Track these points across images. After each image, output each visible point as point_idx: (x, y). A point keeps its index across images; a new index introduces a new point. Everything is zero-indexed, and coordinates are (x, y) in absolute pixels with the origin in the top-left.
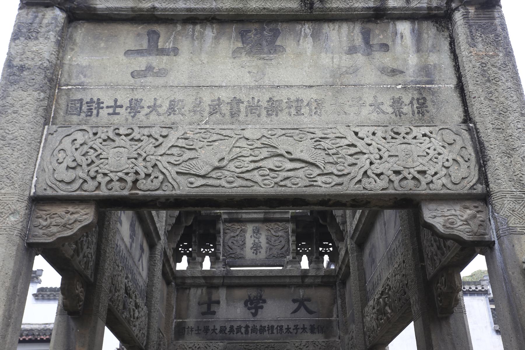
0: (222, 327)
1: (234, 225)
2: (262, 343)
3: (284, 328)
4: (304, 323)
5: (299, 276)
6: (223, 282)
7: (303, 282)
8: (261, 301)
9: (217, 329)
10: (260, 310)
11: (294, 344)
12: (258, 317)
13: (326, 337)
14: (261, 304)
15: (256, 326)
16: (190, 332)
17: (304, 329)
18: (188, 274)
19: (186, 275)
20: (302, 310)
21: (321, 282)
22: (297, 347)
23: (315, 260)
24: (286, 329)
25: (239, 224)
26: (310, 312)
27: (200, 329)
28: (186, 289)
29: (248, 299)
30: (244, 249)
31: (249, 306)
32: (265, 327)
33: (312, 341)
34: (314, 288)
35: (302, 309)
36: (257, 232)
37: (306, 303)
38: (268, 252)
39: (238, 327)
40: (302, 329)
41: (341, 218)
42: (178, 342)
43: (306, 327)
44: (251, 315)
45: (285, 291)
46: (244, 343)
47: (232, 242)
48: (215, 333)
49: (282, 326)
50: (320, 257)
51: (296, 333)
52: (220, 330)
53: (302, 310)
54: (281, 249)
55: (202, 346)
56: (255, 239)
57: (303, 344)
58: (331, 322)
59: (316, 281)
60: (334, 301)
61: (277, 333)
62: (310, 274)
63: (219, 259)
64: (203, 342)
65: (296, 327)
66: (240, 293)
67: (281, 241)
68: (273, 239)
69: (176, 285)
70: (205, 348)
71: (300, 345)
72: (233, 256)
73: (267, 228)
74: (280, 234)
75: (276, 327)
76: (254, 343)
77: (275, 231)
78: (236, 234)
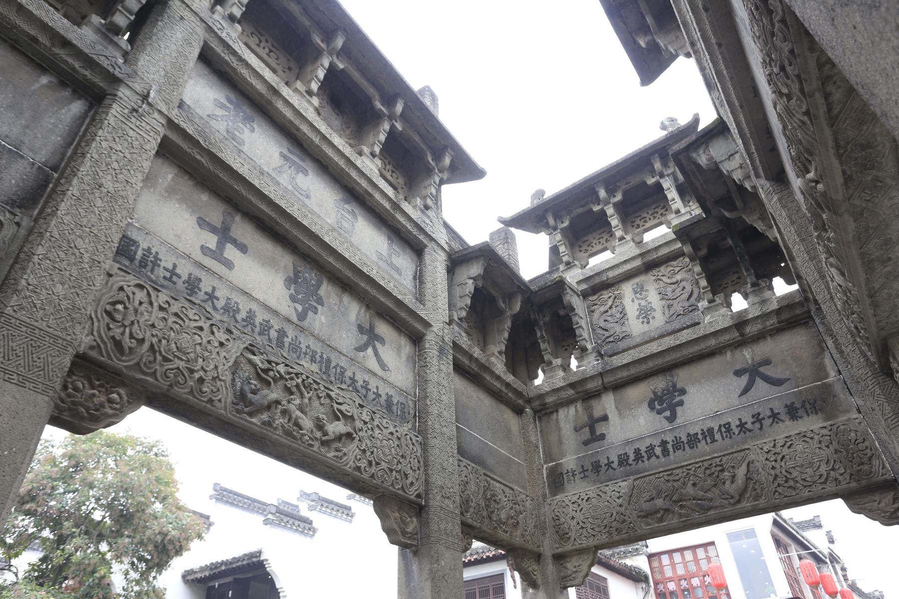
0: (621, 455)
1: (602, 295)
2: (696, 463)
3: (733, 426)
4: (770, 406)
5: (731, 327)
6: (603, 384)
7: (742, 335)
8: (676, 394)
9: (613, 462)
10: (679, 409)
11: (762, 449)
12: (679, 421)
13: (829, 416)
14: (678, 399)
15: (680, 438)
16: (572, 478)
17: (774, 416)
18: (546, 389)
19: (542, 392)
20: (759, 383)
21: (779, 323)
22: (767, 453)
23: (751, 290)
24: (737, 426)
25: (610, 290)
26: (776, 382)
27: (585, 469)
28: (552, 413)
29: (653, 396)
30: (626, 322)
31: (658, 407)
32: (697, 434)
33: (798, 432)
34: (769, 338)
35: (758, 380)
36: (640, 290)
37: (762, 369)
38: (666, 313)
39: (647, 448)
40: (769, 417)
41: (739, 171)
42: (555, 498)
43: (776, 411)
44: (667, 425)
45: (717, 361)
46: (663, 472)
47: (605, 321)
48: (612, 468)
49: (729, 423)
50: (760, 281)
51: (761, 429)
52: (619, 461)
53: (759, 383)
54: (689, 299)
55: (591, 495)
56: (640, 301)
57: (781, 443)
58: (827, 388)
59: (768, 323)
60: (821, 347)
61: (723, 439)
62: (750, 316)
63: (587, 350)
64: (593, 488)
65: (758, 418)
66: (640, 392)
67: (684, 288)
68: (669, 289)
69: (536, 412)
70: (598, 497)
71: (774, 446)
72: (611, 339)
73: (654, 278)
74: (678, 277)
75: (716, 429)
76: (682, 467)
77: (669, 278)
78: (608, 306)
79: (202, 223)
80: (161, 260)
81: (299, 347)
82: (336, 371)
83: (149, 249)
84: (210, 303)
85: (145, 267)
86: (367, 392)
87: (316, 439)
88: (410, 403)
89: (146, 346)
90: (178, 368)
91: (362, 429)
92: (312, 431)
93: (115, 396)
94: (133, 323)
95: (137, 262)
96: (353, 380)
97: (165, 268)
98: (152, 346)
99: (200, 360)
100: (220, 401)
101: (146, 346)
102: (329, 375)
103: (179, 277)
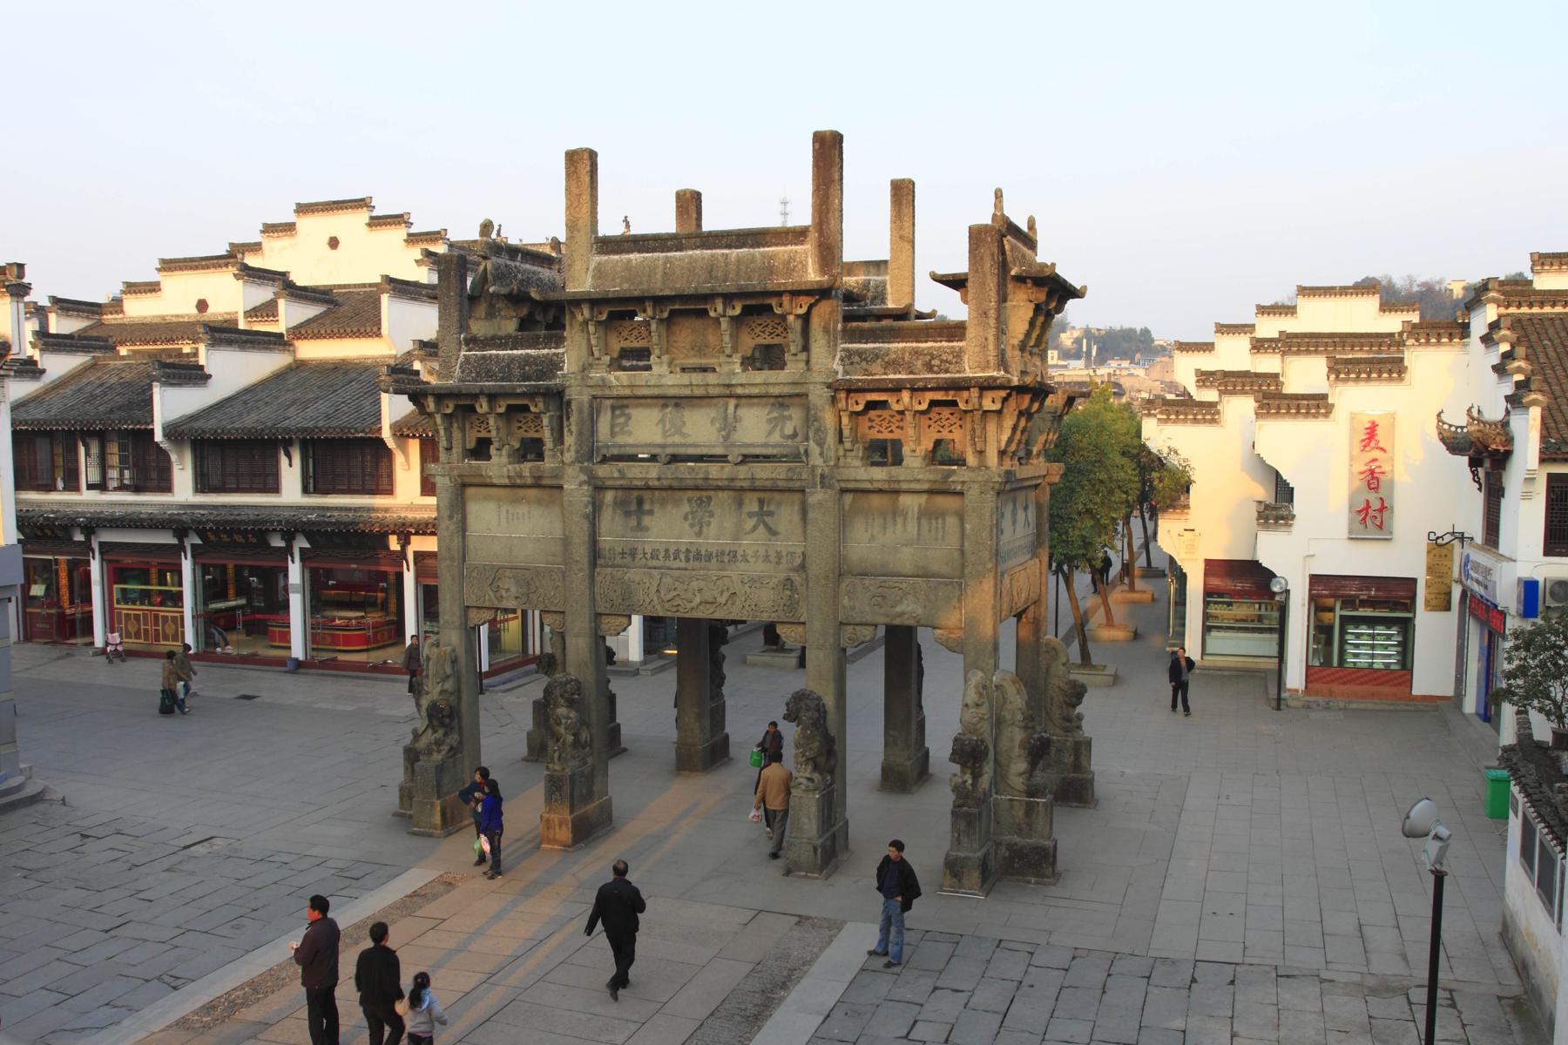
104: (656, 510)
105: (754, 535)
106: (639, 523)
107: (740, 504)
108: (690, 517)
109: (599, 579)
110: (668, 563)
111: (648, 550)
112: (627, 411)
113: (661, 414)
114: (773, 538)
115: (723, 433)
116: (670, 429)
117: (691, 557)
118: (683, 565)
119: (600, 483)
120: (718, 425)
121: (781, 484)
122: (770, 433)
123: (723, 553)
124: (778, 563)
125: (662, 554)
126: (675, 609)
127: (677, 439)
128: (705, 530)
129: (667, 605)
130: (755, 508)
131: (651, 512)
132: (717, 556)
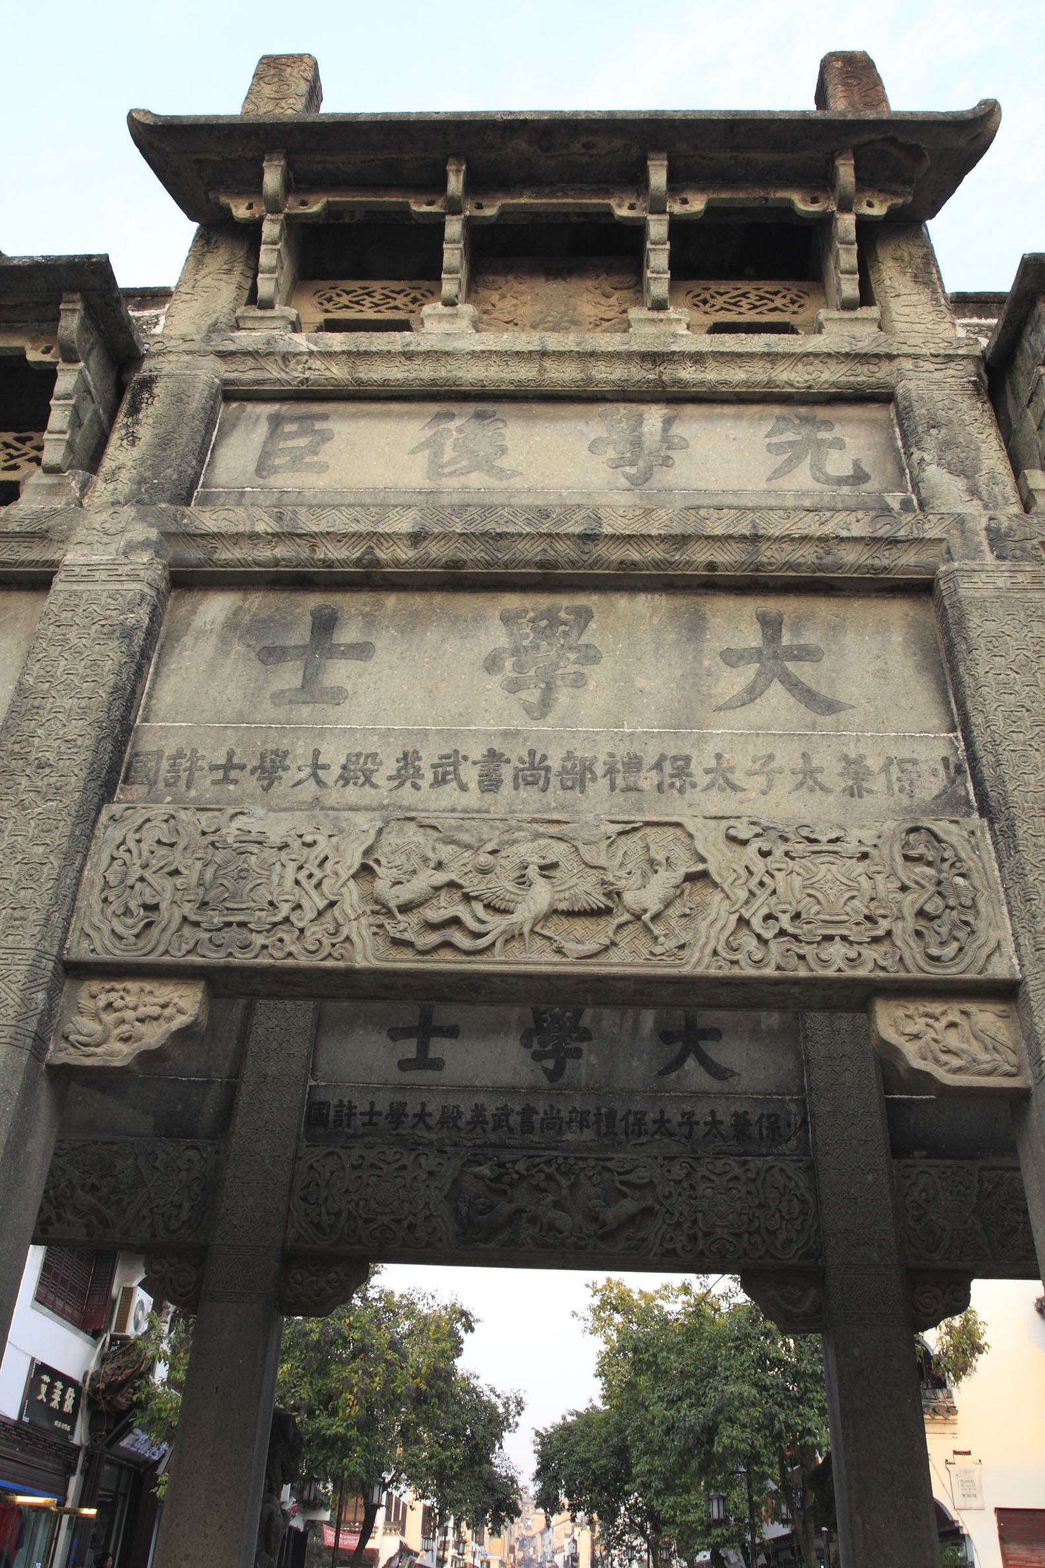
79: (396, 1034)
80: (355, 1107)
81: (558, 1118)
82: (627, 1122)
83: (341, 1101)
84: (421, 1125)
85: (340, 1125)
86: (691, 1128)
87: (589, 1236)
88: (793, 1108)
89: (344, 1215)
90: (383, 1225)
91: (671, 1194)
92: (580, 1227)
93: (332, 1275)
94: (326, 1199)
95: (331, 1125)
96: (661, 1122)
97: (362, 1114)
98: (350, 1213)
99: (407, 1204)
100: (440, 1240)
101: (344, 1215)
102: (615, 1134)
103: (379, 1114)
104: (378, 644)
105: (755, 713)
106: (309, 682)
107: (696, 628)
108: (509, 663)
109: (109, 835)
110: (407, 795)
111: (334, 756)
112: (318, 426)
113: (429, 433)
114: (829, 720)
115: (633, 470)
116: (454, 461)
117: (507, 772)
118: (473, 798)
119: (194, 554)
120: (611, 453)
121: (850, 556)
122: (778, 473)
123: (634, 763)
124: (853, 792)
125: (390, 766)
126: (433, 938)
127: (476, 480)
128: (563, 697)
129: (407, 926)
130: (751, 637)
131: (362, 651)
132: (611, 771)
